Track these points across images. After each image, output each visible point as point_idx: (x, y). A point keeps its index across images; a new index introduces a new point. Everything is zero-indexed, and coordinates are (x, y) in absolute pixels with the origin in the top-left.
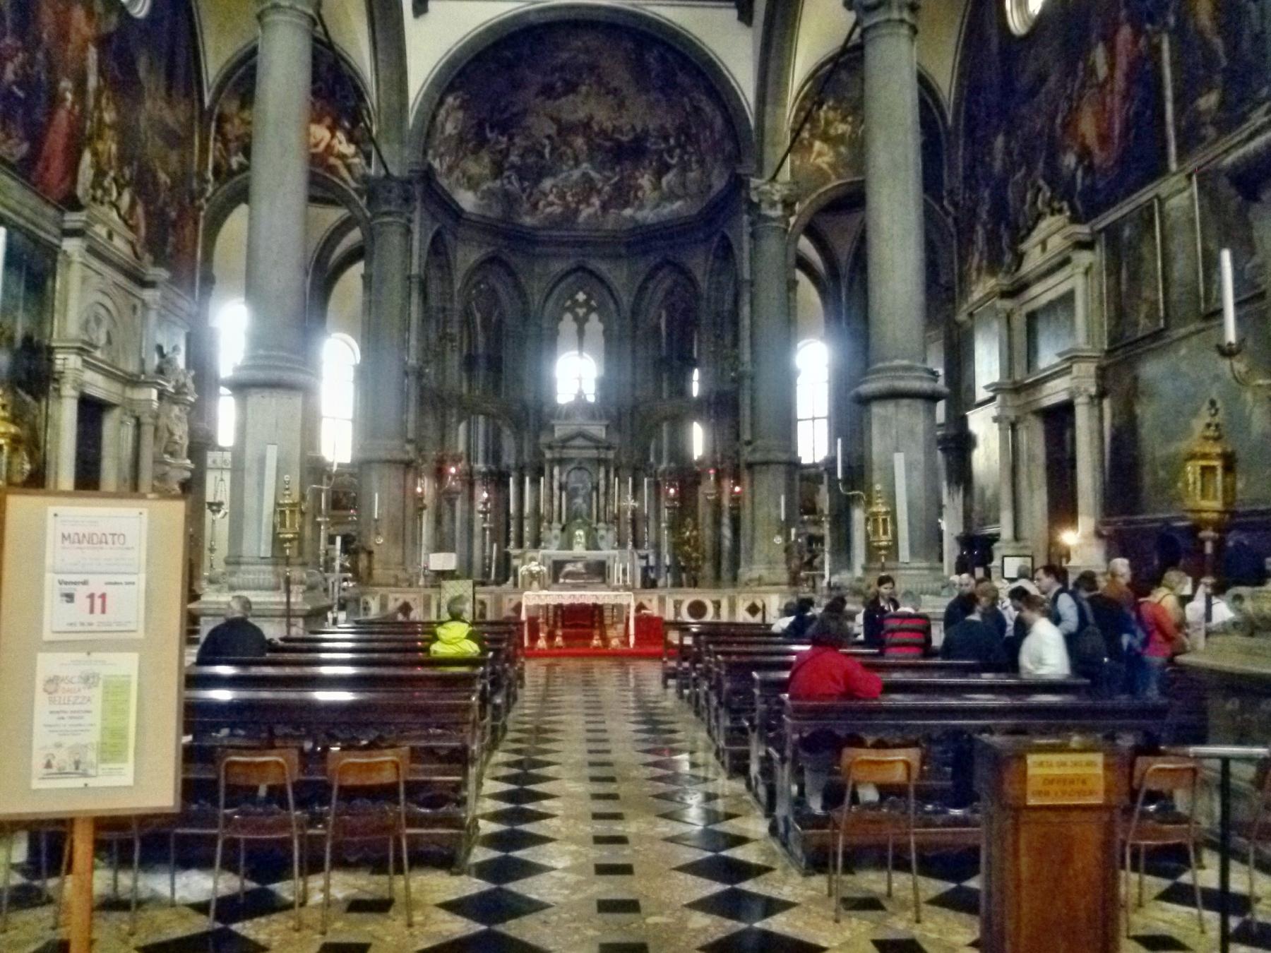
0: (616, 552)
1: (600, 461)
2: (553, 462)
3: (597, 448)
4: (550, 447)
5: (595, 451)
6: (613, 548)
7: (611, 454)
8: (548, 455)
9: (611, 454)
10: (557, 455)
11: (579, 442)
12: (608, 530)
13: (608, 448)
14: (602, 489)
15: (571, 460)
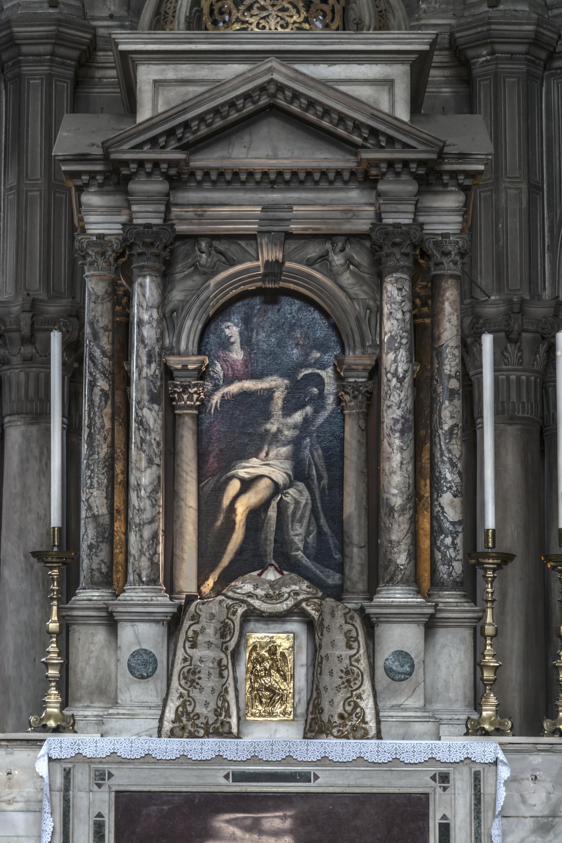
0: (486, 749)
1: (379, 248)
2: (125, 257)
3: (366, 178)
4: (116, 177)
5: (354, 195)
6: (475, 729)
7: (444, 215)
8: (100, 218)
9: (444, 215)
10: (147, 215)
11: (268, 149)
12: (431, 625)
13: (430, 176)
14: (395, 404)
15: (229, 244)
